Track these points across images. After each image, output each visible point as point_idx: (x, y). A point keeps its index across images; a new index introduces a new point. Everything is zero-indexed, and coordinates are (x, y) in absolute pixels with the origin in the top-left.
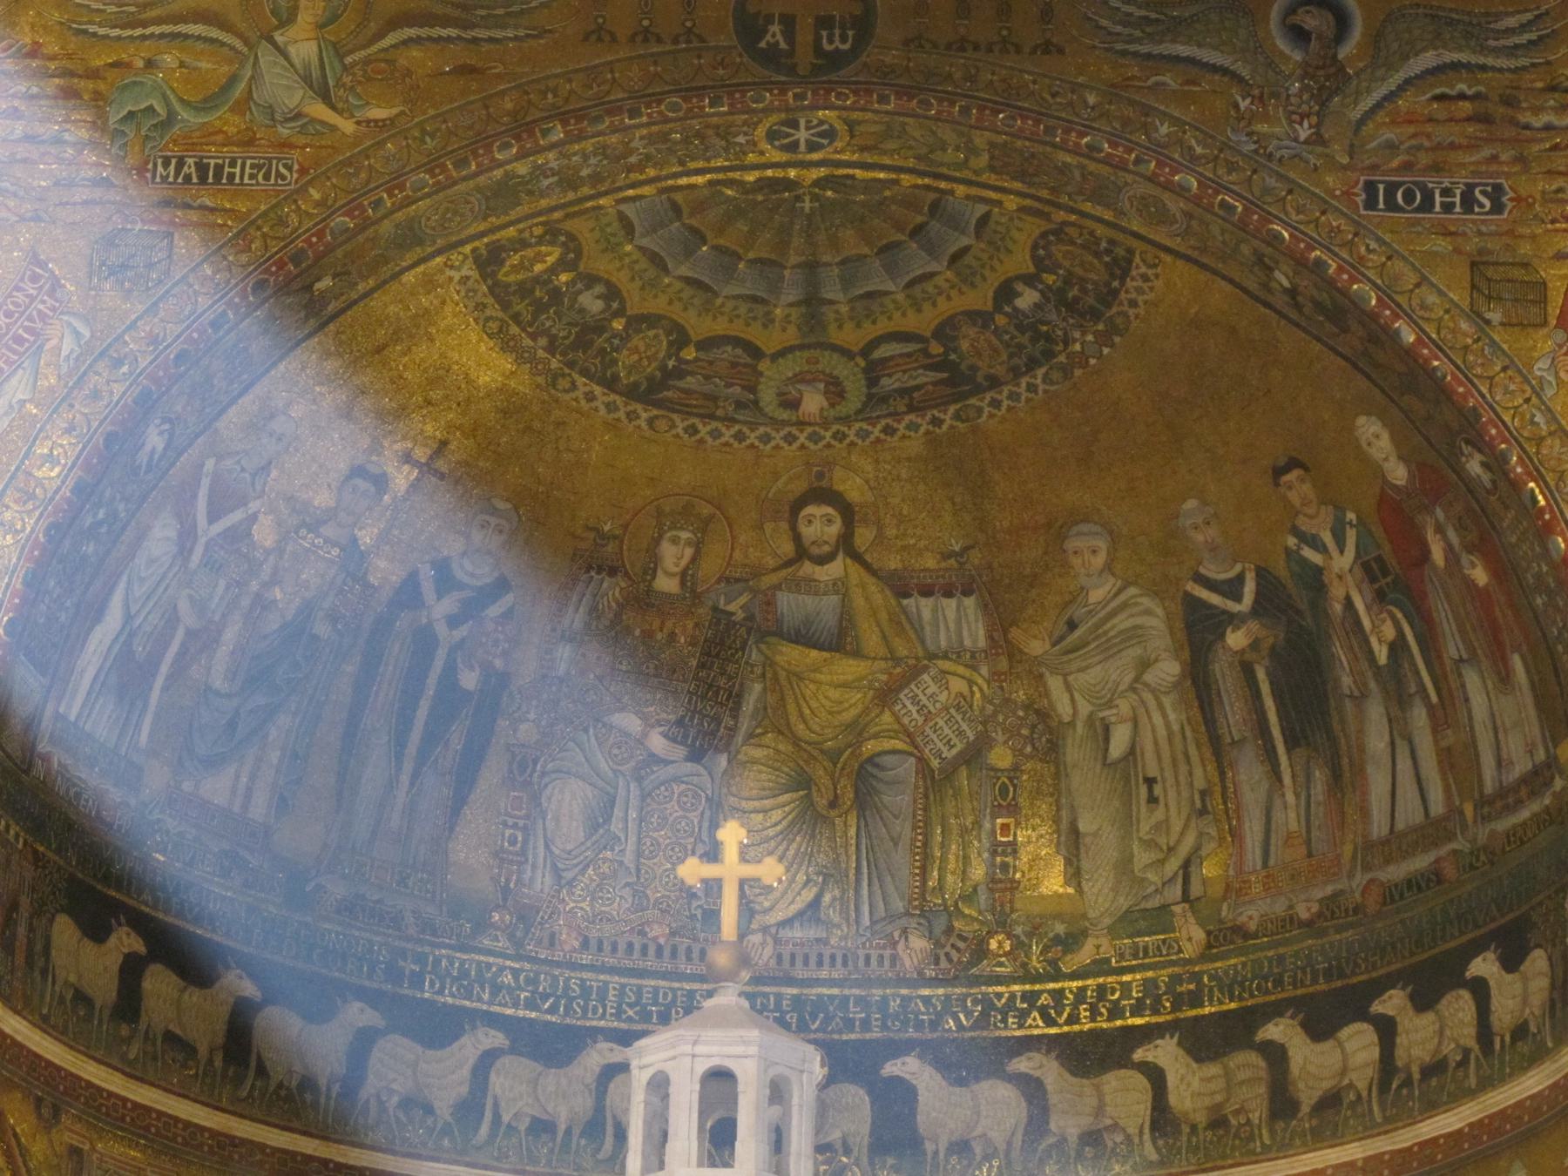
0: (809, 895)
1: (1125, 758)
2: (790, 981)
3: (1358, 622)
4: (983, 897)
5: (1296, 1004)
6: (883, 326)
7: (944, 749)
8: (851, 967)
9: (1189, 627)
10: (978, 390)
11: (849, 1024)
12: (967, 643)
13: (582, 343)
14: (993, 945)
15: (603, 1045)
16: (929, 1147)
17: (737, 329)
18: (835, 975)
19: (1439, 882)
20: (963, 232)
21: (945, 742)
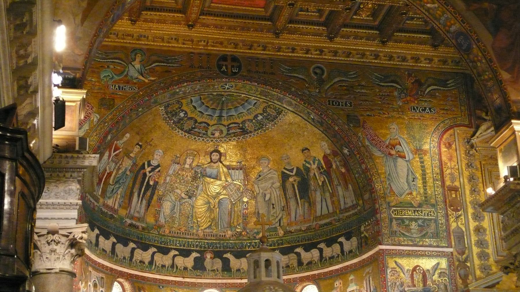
0: (209, 224)
3: (316, 177)
4: (241, 224)
5: (302, 245)
6: (232, 121)
10: (248, 133)
11: (217, 247)
12: (240, 178)
13: (179, 122)
14: (243, 233)
15: (173, 251)
16: (233, 270)
17: (206, 121)
18: (214, 238)
19: (331, 224)
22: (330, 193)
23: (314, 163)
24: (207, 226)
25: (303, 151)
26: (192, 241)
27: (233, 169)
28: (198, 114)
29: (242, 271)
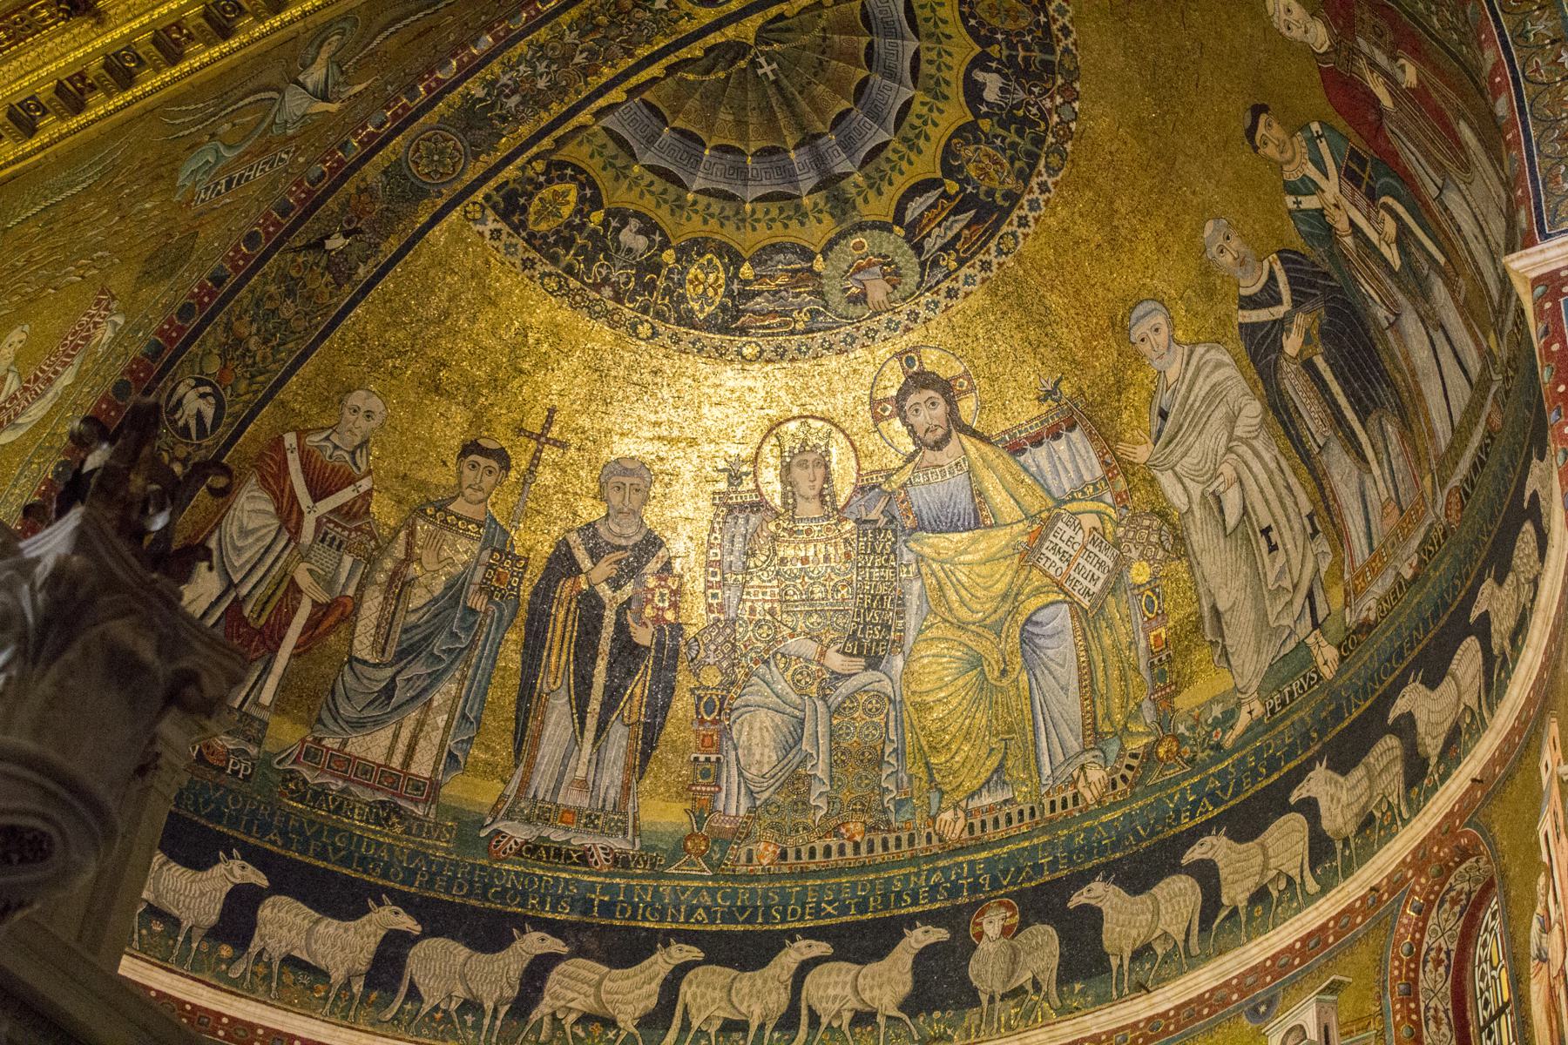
0: (993, 762)
1: (1241, 521)
2: (984, 846)
6: (901, 184)
7: (1090, 586)
8: (1038, 817)
9: (1253, 361)
11: (1039, 869)
12: (1087, 477)
14: (1162, 751)
15: (802, 944)
16: (1114, 962)
20: (903, 38)
21: (1090, 577)
24: (984, 776)
26: (907, 877)
27: (1037, 442)
29: (1159, 951)
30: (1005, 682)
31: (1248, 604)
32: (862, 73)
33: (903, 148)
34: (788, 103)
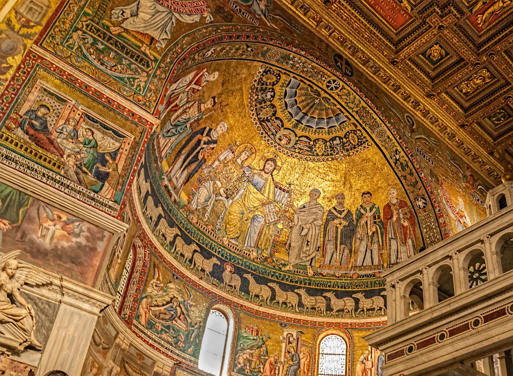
0: (237, 235)
2: (230, 250)
3: (367, 226)
6: (307, 134)
11: (238, 263)
14: (269, 260)
16: (251, 294)
21: (272, 218)
22: (379, 245)
23: (371, 210)
25: (364, 194)
26: (215, 245)
27: (280, 189)
28: (283, 106)
30: (245, 222)
31: (297, 249)
32: (325, 117)
33: (314, 131)
34: (311, 107)
